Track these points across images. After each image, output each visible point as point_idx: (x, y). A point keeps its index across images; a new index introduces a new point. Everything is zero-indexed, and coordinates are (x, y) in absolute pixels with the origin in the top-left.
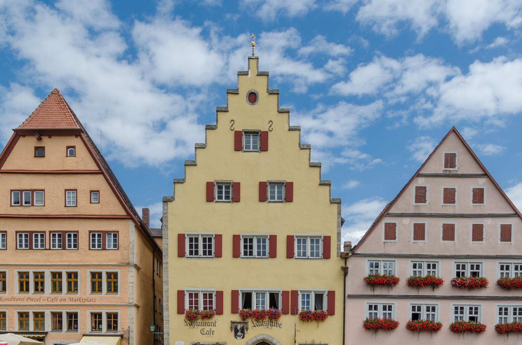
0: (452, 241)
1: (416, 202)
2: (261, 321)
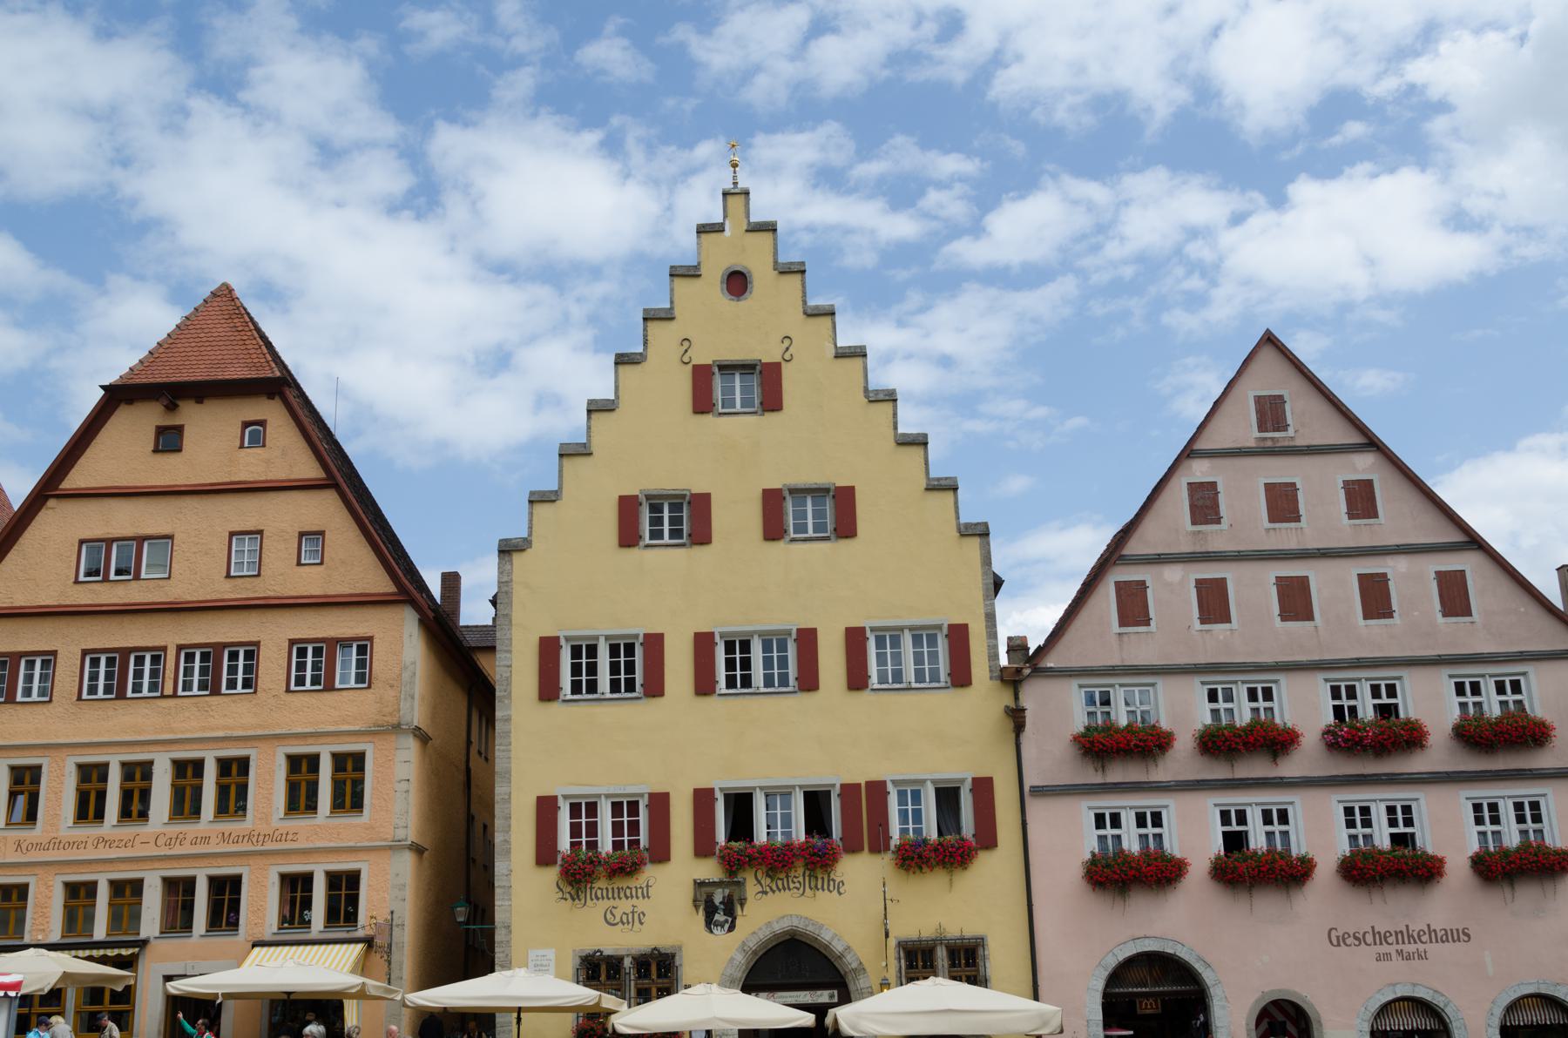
0: (1307, 623)
1: (1194, 523)
2: (782, 876)
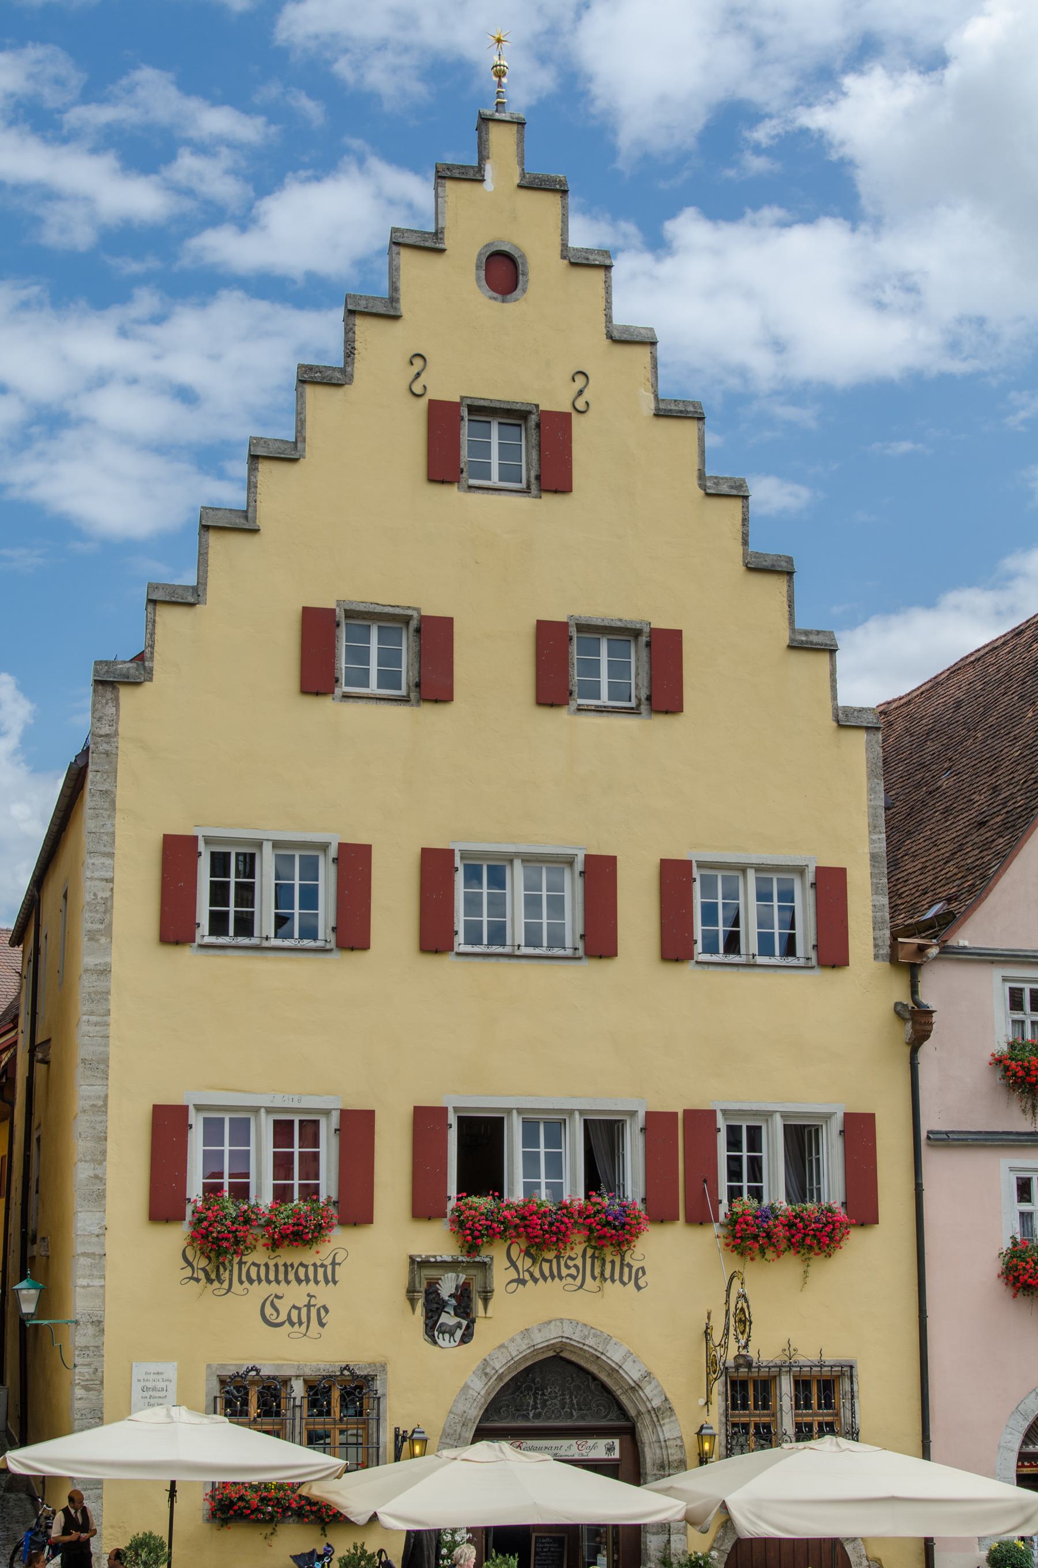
2: (551, 1255)
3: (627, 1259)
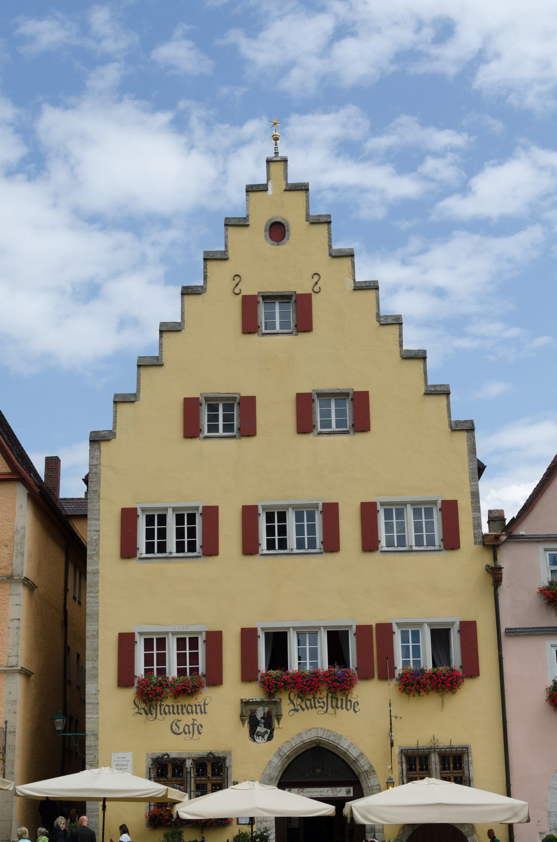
2: (310, 697)
3: (349, 698)
